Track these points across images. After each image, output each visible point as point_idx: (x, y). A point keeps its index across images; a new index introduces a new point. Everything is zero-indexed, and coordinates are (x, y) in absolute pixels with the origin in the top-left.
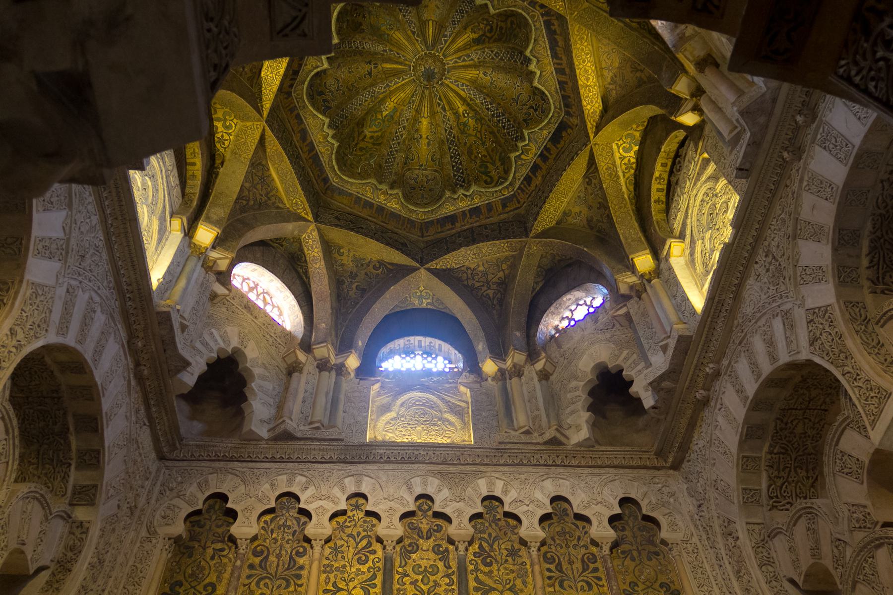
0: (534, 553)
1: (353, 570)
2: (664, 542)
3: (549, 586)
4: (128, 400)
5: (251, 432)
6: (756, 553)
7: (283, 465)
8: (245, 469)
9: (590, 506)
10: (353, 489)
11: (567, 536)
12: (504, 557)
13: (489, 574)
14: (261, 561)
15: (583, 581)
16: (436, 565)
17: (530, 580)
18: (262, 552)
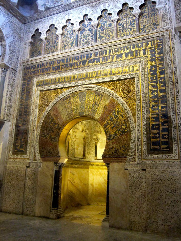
0: (115, 24)
1: (69, 40)
2: (157, 9)
3: (119, 32)
4: (2, 12)
5: (40, 10)
6: (175, 6)
7: (50, 17)
8: (42, 21)
9: (134, 4)
10: (67, 19)
11: (127, 16)
12: (107, 27)
13: (103, 33)
14: (49, 43)
15: (129, 28)
16: (89, 34)
17: (113, 32)
18: (49, 41)
